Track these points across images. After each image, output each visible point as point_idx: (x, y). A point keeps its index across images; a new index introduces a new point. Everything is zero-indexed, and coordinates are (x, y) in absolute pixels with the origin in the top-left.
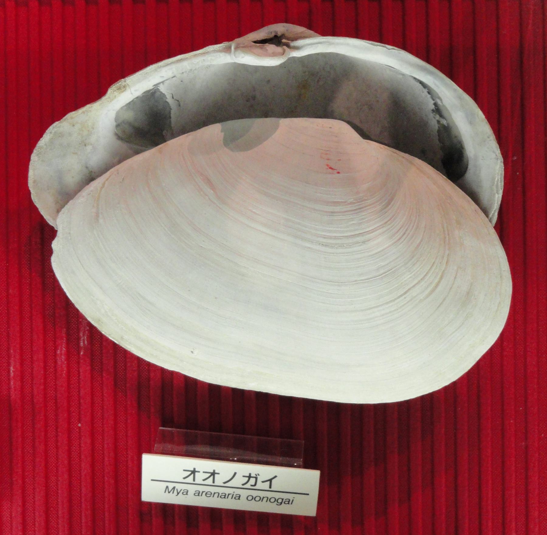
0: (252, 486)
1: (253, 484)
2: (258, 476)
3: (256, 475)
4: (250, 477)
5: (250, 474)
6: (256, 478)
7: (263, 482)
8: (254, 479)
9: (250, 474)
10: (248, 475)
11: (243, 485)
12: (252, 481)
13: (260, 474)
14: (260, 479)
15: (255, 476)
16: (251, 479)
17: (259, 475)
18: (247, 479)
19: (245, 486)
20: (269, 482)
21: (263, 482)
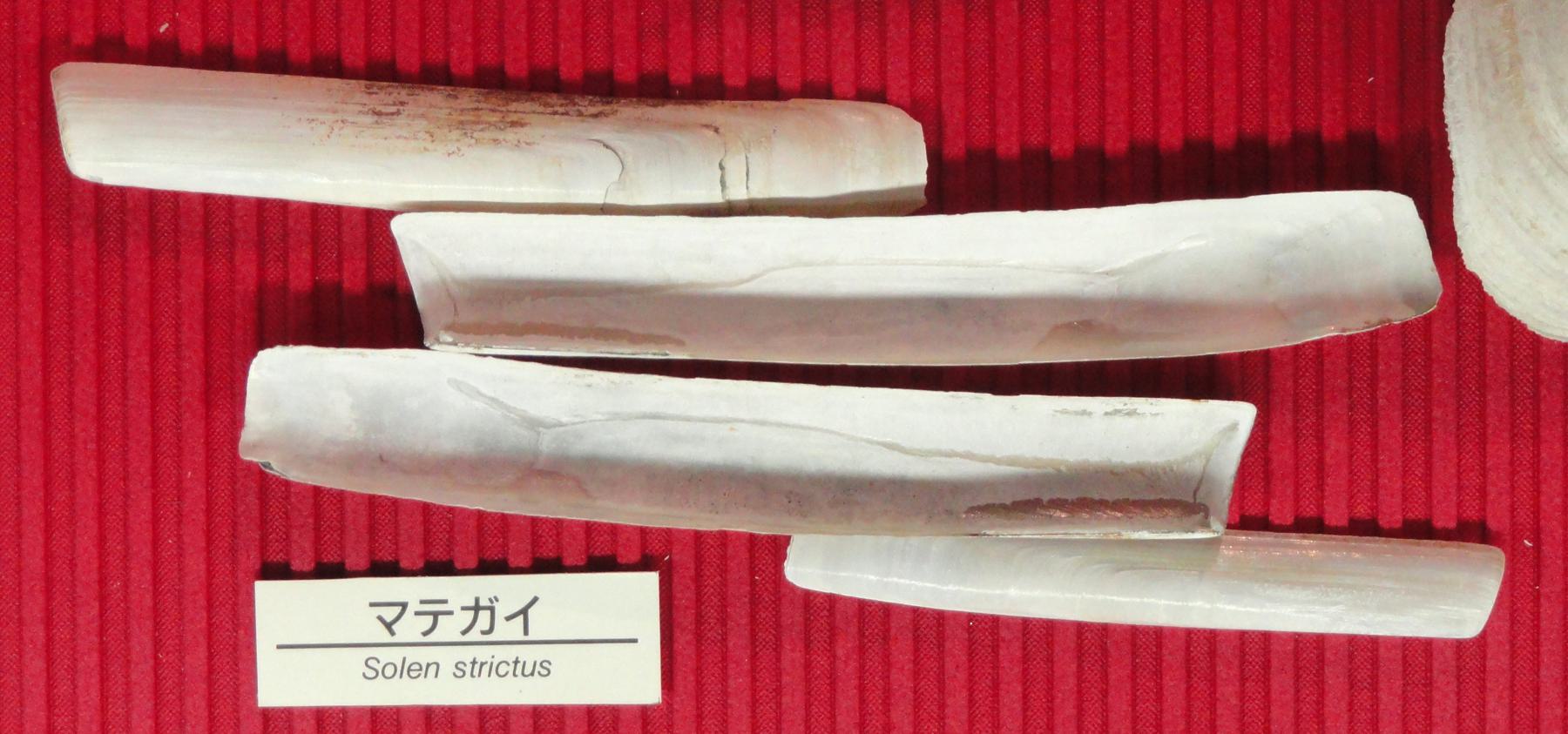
0: (483, 633)
1: (487, 627)
2: (495, 604)
3: (490, 600)
4: (477, 608)
5: (477, 600)
6: (492, 609)
7: (508, 618)
8: (488, 612)
9: (477, 600)
10: (472, 604)
11: (464, 633)
12: (484, 618)
13: (499, 597)
14: (502, 612)
15: (489, 604)
16: (481, 613)
17: (497, 600)
18: (472, 613)
19: (467, 638)
20: (521, 617)
21: (508, 618)
